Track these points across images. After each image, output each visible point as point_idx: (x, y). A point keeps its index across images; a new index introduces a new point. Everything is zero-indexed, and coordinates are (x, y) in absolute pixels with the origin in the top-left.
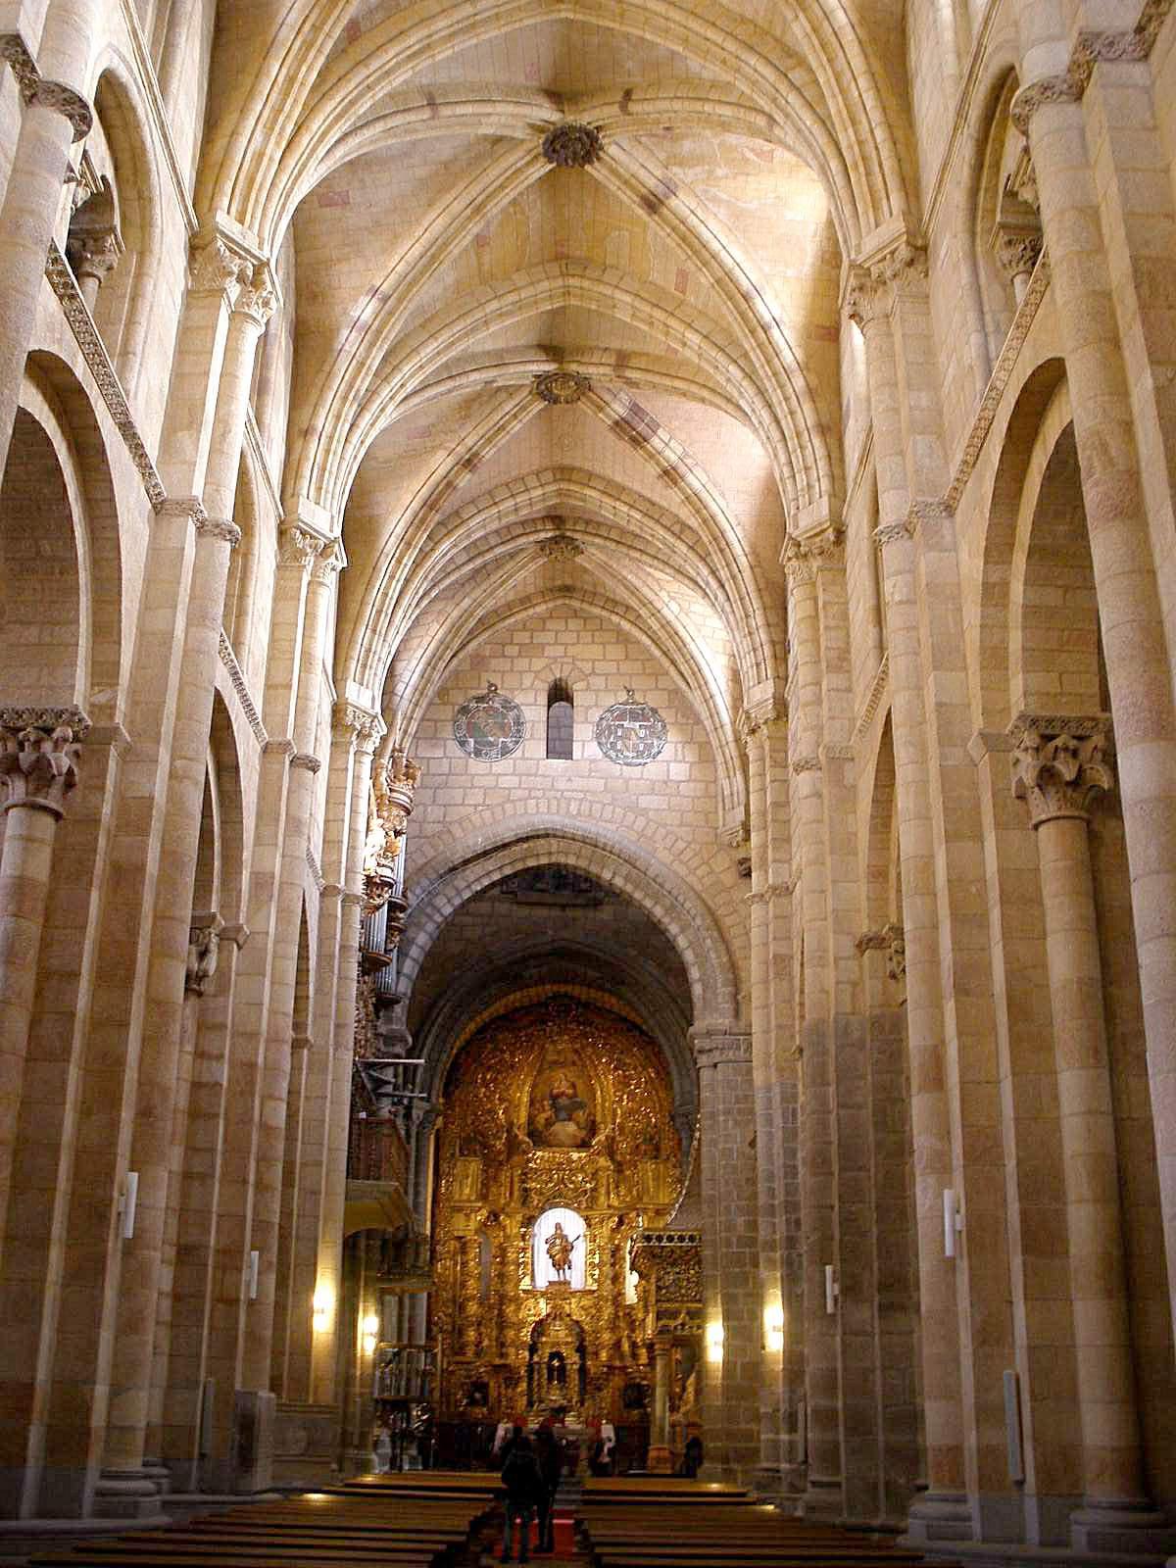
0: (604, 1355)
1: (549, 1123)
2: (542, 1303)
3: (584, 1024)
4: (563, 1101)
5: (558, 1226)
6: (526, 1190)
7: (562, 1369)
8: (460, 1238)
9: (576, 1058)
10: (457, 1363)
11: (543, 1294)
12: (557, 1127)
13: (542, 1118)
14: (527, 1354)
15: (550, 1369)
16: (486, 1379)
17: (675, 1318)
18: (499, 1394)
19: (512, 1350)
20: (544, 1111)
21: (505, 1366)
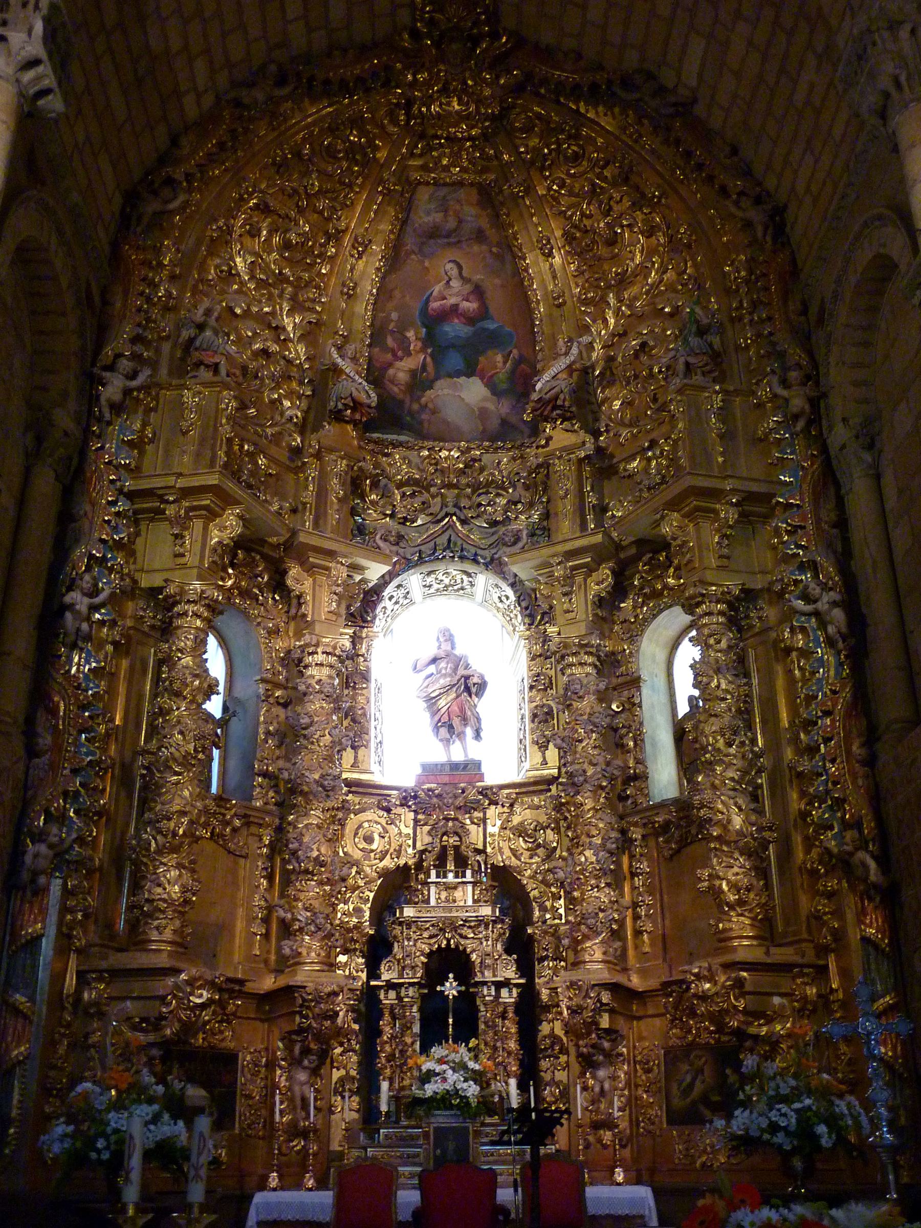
4: (455, 329)
8: (154, 592)
9: (484, 223)
10: (116, 974)
11: (408, 798)
13: (401, 371)
21: (289, 991)
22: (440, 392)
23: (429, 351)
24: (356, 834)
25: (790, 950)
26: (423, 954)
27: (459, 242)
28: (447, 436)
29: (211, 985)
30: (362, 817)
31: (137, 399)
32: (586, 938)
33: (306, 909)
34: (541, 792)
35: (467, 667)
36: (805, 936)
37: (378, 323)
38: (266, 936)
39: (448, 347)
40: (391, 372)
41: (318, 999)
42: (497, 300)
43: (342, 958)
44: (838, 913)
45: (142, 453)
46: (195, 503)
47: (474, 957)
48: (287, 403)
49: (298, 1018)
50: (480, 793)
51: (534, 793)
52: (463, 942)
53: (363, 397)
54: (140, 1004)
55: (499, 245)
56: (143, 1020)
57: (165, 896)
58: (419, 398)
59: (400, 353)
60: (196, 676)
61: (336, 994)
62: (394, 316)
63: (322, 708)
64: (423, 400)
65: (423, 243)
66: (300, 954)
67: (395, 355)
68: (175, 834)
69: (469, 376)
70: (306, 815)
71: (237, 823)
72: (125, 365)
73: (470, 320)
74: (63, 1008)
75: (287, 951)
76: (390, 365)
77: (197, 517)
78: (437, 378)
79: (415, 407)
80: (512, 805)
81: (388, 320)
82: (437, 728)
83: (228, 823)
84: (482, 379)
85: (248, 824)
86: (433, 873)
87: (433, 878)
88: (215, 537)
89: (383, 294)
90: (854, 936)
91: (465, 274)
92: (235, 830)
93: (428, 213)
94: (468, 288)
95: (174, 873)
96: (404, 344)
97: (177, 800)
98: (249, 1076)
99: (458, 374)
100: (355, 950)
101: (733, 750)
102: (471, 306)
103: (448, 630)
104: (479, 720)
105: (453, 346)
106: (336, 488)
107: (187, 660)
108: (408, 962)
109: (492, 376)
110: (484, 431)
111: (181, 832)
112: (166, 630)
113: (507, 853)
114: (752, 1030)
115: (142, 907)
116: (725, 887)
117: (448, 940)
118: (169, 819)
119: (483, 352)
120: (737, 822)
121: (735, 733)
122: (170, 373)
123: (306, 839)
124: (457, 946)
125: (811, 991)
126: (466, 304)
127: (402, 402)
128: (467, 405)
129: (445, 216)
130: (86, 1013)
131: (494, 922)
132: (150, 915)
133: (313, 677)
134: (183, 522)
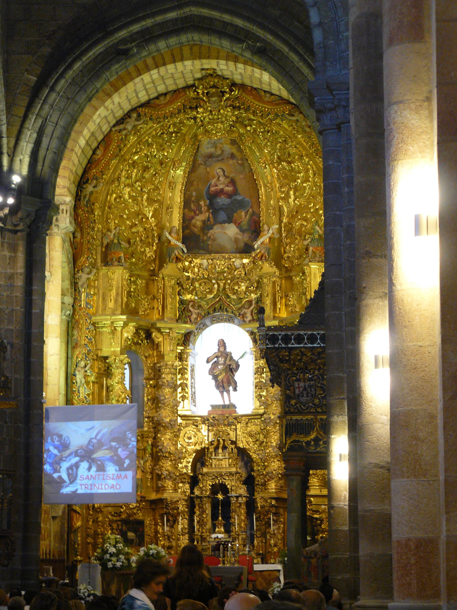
0: (272, 486)
1: (207, 226)
2: (204, 428)
3: (239, 108)
4: (222, 200)
5: (222, 344)
6: (182, 302)
7: (227, 503)
9: (234, 151)
11: (204, 420)
12: (217, 230)
13: (198, 220)
14: (187, 486)
15: (215, 504)
16: (140, 516)
17: (308, 433)
18: (157, 532)
19: (169, 484)
20: (202, 213)
21: (161, 501)
22: (216, 231)
23: (211, 211)
24: (184, 436)
26: (210, 485)
27: (223, 159)
28: (220, 250)
30: (187, 429)
32: (269, 480)
33: (166, 471)
34: (258, 419)
35: (231, 358)
37: (187, 197)
38: (152, 479)
39: (220, 209)
40: (194, 221)
41: (172, 503)
42: (242, 184)
43: (181, 485)
47: (228, 487)
48: (147, 250)
49: (165, 510)
50: (235, 419)
51: (255, 419)
52: (224, 481)
54: (114, 508)
55: (242, 159)
56: (115, 513)
58: (206, 234)
59: (197, 212)
61: (178, 501)
62: (194, 194)
64: (209, 235)
65: (206, 161)
66: (164, 487)
67: (195, 213)
69: (229, 223)
70: (165, 434)
72: (87, 270)
73: (229, 196)
74: (90, 510)
75: (160, 485)
76: (193, 218)
78: (214, 225)
79: (205, 238)
80: (247, 423)
81: (191, 196)
82: (218, 387)
84: (235, 224)
86: (214, 454)
87: (213, 457)
89: (188, 184)
91: (226, 174)
93: (208, 148)
94: (228, 181)
96: (199, 207)
98: (148, 528)
99: (224, 222)
100: (185, 482)
102: (229, 189)
103: (223, 340)
104: (236, 383)
105: (221, 209)
108: (204, 488)
109: (240, 222)
110: (237, 248)
113: (245, 443)
114: (316, 516)
117: (219, 480)
119: (236, 211)
123: (165, 444)
124: (222, 482)
126: (227, 188)
127: (199, 236)
128: (229, 237)
129: (216, 150)
130: (96, 511)
131: (236, 473)
133: (164, 378)
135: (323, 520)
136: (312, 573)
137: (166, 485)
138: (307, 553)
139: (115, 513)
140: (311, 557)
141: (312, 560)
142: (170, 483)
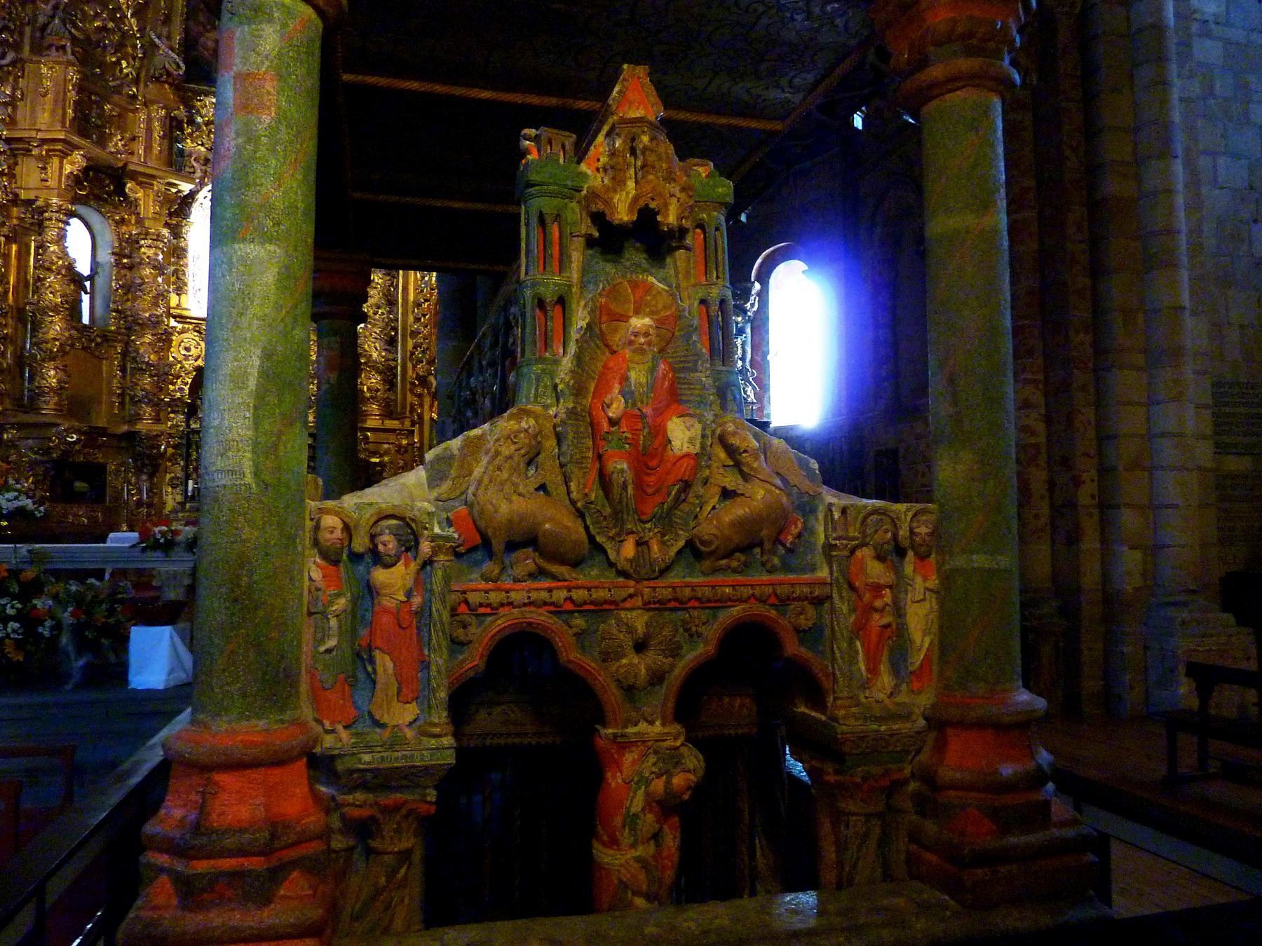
8: (30, 202)
10: (21, 426)
25: (397, 422)
29: (78, 432)
31: (9, 73)
33: (142, 390)
36: (408, 414)
40: (202, 39)
41: (148, 437)
44: (421, 406)
45: (15, 108)
46: (52, 147)
48: (124, 64)
53: (172, 68)
57: (48, 385)
60: (59, 258)
63: (151, 273)
66: (139, 414)
67: (204, 27)
68: (51, 351)
71: (99, 340)
76: (202, 34)
77: (57, 156)
83: (91, 341)
85: (107, 341)
88: (68, 168)
90: (426, 417)
92: (97, 344)
95: (52, 373)
97: (52, 332)
101: (377, 317)
106: (157, 132)
107: (53, 248)
111: (55, 350)
112: (40, 227)
114: (373, 460)
115: (34, 391)
116: (365, 390)
118: (47, 343)
120: (375, 355)
121: (378, 308)
122: (32, 51)
123: (141, 351)
125: (404, 442)
132: (39, 395)
134: (44, 161)
135: (385, 466)
136: (384, 664)
137: (142, 412)
138: (347, 528)
139: (39, 449)
140: (378, 558)
141: (380, 575)
142: (149, 410)
